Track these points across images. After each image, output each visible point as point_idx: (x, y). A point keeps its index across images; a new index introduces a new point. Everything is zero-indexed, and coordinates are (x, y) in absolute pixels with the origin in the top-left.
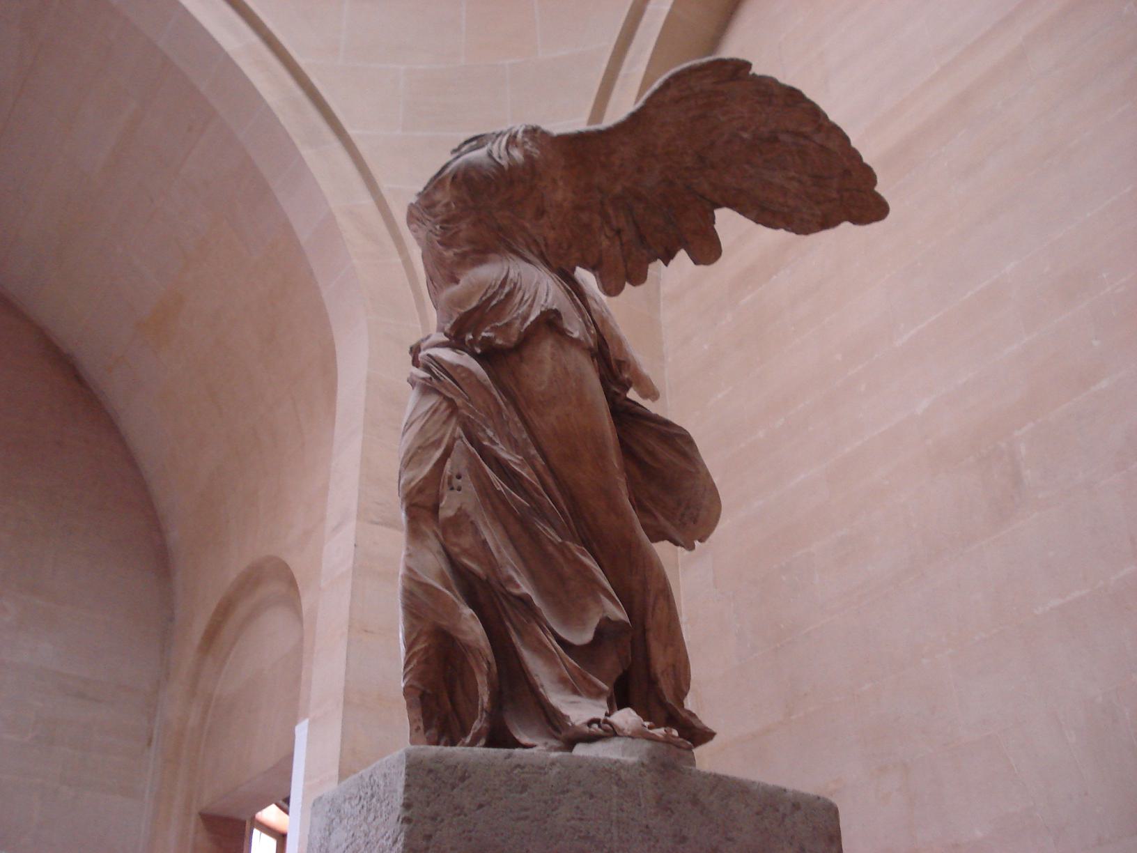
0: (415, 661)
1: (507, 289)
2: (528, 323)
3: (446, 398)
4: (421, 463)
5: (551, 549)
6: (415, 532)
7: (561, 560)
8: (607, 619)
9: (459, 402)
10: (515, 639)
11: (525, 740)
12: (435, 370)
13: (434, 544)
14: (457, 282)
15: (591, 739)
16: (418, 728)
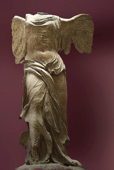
0: (37, 141)
1: (57, 61)
2: (61, 71)
3: (45, 82)
4: (40, 97)
5: (60, 123)
6: (38, 112)
7: (61, 125)
8: (68, 140)
9: (48, 85)
10: (55, 140)
11: (55, 161)
12: (43, 75)
13: (41, 116)
14: (43, 52)
15: (72, 165)
16: (36, 154)
